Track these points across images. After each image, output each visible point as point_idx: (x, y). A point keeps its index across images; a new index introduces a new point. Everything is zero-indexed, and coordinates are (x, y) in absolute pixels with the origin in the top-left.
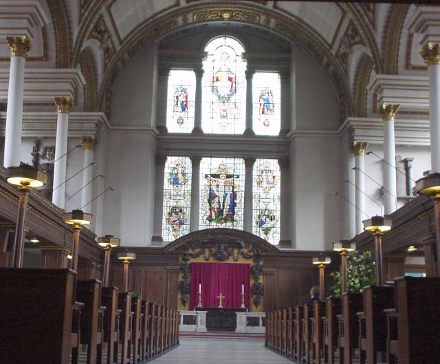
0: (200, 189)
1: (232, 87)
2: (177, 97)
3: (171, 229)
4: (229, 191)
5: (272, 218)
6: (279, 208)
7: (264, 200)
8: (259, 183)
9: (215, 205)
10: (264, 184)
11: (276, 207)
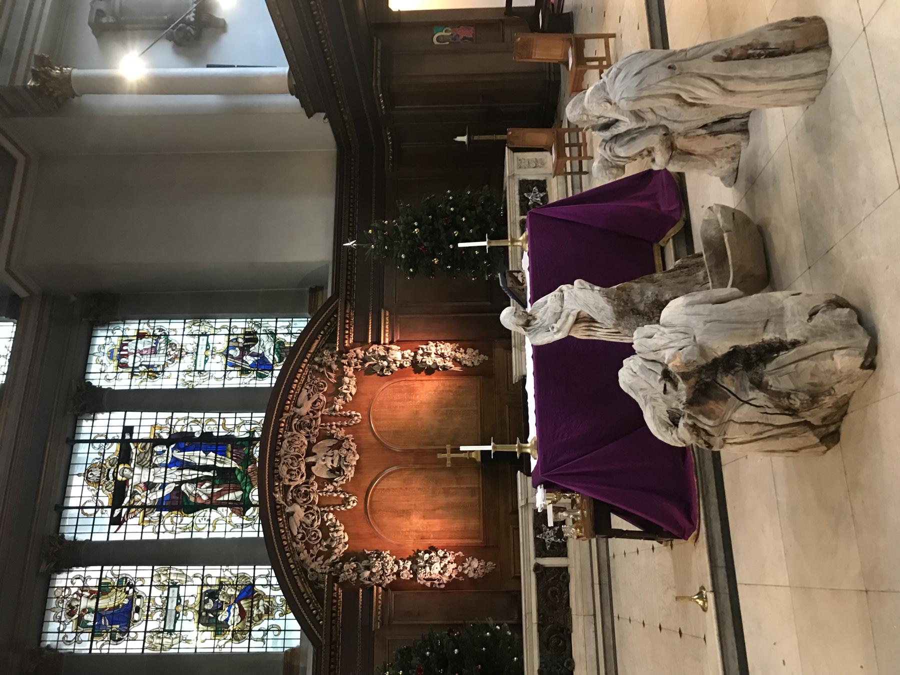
0: (154, 537)
3: (264, 625)
5: (251, 338)
6: (221, 323)
7: (201, 358)
8: (152, 372)
9: (204, 492)
10: (158, 360)
11: (221, 331)
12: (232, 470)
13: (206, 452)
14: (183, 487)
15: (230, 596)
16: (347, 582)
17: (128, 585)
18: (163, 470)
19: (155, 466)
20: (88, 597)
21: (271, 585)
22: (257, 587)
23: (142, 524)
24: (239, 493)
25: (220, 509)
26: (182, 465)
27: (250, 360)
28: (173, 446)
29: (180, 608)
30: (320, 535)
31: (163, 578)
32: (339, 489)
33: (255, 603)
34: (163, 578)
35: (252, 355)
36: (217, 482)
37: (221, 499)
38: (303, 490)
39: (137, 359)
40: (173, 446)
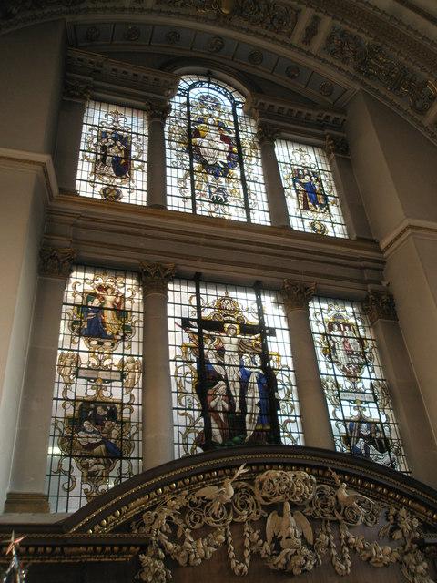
0: (172, 357)
1: (230, 151)
2: (104, 148)
3: (76, 472)
4: (253, 363)
8: (330, 352)
10: (341, 354)
12: (244, 431)
13: (259, 404)
14: (222, 382)
15: (109, 433)
16: (139, 566)
17: (125, 335)
18: (237, 364)
19: (240, 356)
20: (115, 302)
21: (120, 478)
22: (119, 462)
23: (184, 346)
24: (220, 439)
25: (202, 420)
26: (244, 381)
27: (361, 444)
28: (261, 371)
29: (99, 383)
30: (198, 526)
31: (130, 366)
32: (254, 549)
33: (101, 460)
34: (130, 366)
35: (366, 448)
36: (230, 416)
37: (212, 420)
38: (250, 500)
39: (339, 339)
40: (261, 371)
